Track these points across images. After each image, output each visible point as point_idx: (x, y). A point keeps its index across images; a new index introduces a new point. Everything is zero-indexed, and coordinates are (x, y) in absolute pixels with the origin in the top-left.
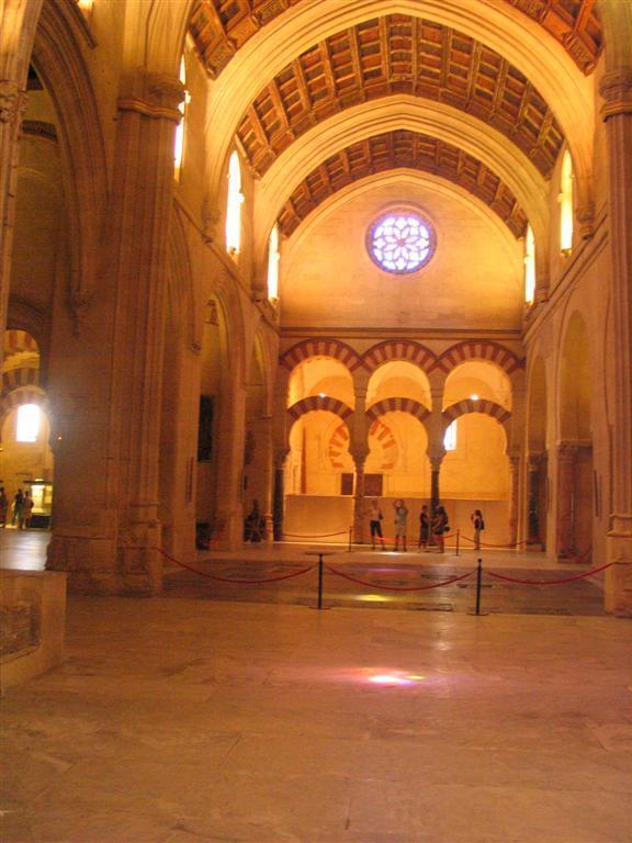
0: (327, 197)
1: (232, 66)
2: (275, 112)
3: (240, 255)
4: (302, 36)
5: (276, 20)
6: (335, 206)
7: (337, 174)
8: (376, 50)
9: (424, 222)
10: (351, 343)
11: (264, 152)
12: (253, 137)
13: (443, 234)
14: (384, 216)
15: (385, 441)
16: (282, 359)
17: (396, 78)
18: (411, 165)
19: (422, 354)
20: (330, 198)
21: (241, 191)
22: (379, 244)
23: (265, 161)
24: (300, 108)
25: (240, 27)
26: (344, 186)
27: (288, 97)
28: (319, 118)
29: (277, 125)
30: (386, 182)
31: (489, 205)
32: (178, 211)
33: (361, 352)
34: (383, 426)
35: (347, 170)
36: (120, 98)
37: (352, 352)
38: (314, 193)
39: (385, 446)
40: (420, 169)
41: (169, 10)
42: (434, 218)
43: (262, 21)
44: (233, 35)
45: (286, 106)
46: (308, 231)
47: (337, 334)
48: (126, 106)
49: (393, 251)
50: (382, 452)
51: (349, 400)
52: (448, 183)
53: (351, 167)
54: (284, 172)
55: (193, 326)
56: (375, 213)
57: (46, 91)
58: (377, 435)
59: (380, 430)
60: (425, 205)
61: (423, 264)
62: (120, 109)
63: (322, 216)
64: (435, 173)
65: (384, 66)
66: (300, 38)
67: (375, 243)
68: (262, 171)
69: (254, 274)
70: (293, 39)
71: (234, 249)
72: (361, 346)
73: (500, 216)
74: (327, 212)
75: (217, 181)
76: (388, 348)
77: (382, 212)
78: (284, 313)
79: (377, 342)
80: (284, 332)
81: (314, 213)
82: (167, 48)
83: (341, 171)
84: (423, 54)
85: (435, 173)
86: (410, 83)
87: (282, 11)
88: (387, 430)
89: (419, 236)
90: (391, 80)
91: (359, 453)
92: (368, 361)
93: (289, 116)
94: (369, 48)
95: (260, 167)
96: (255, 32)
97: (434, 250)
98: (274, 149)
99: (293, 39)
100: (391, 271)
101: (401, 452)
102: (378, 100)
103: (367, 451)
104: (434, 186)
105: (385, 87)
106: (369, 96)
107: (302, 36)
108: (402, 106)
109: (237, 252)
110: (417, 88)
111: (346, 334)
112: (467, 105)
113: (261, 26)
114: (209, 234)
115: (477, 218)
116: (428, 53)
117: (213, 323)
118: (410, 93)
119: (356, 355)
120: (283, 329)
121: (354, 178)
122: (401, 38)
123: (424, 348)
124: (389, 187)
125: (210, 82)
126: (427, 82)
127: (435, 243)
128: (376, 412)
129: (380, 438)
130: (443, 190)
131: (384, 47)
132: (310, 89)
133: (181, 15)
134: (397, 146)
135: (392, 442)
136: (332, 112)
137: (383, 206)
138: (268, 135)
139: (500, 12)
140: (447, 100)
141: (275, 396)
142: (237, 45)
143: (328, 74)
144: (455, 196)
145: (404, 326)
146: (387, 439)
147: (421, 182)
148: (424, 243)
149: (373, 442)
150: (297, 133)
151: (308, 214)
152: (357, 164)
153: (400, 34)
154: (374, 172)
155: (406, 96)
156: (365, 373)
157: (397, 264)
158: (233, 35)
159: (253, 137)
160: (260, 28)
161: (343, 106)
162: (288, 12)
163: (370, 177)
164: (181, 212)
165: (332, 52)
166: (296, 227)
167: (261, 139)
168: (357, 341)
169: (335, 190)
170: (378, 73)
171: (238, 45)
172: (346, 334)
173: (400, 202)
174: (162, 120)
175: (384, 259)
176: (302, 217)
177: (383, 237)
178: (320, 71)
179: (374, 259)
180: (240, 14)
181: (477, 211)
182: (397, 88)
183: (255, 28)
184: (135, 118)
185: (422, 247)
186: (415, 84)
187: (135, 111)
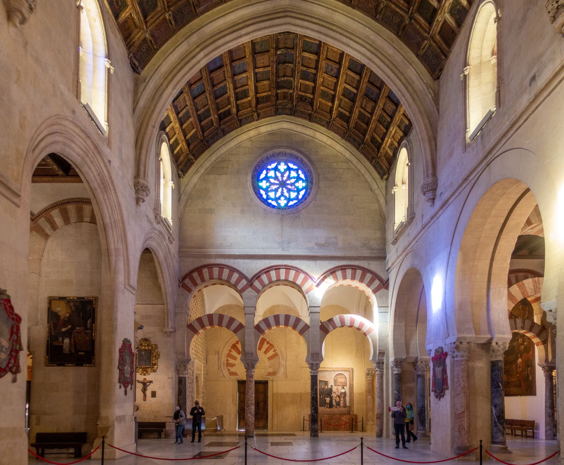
0: (217, 140)
15: (271, 353)
31: (358, 149)
34: (268, 343)
39: (270, 358)
50: (267, 363)
51: (240, 319)
52: (323, 129)
58: (264, 349)
59: (265, 346)
67: (261, 184)
73: (368, 159)
88: (271, 346)
91: (250, 364)
100: (274, 207)
101: (283, 363)
103: (257, 360)
119: (246, 278)
128: (263, 326)
129: (266, 352)
130: (318, 136)
135: (276, 355)
137: (266, 151)
141: (176, 314)
146: (271, 353)
148: (301, 185)
149: (261, 354)
156: (255, 294)
157: (279, 201)
163: (255, 123)
177: (267, 178)
179: (260, 196)
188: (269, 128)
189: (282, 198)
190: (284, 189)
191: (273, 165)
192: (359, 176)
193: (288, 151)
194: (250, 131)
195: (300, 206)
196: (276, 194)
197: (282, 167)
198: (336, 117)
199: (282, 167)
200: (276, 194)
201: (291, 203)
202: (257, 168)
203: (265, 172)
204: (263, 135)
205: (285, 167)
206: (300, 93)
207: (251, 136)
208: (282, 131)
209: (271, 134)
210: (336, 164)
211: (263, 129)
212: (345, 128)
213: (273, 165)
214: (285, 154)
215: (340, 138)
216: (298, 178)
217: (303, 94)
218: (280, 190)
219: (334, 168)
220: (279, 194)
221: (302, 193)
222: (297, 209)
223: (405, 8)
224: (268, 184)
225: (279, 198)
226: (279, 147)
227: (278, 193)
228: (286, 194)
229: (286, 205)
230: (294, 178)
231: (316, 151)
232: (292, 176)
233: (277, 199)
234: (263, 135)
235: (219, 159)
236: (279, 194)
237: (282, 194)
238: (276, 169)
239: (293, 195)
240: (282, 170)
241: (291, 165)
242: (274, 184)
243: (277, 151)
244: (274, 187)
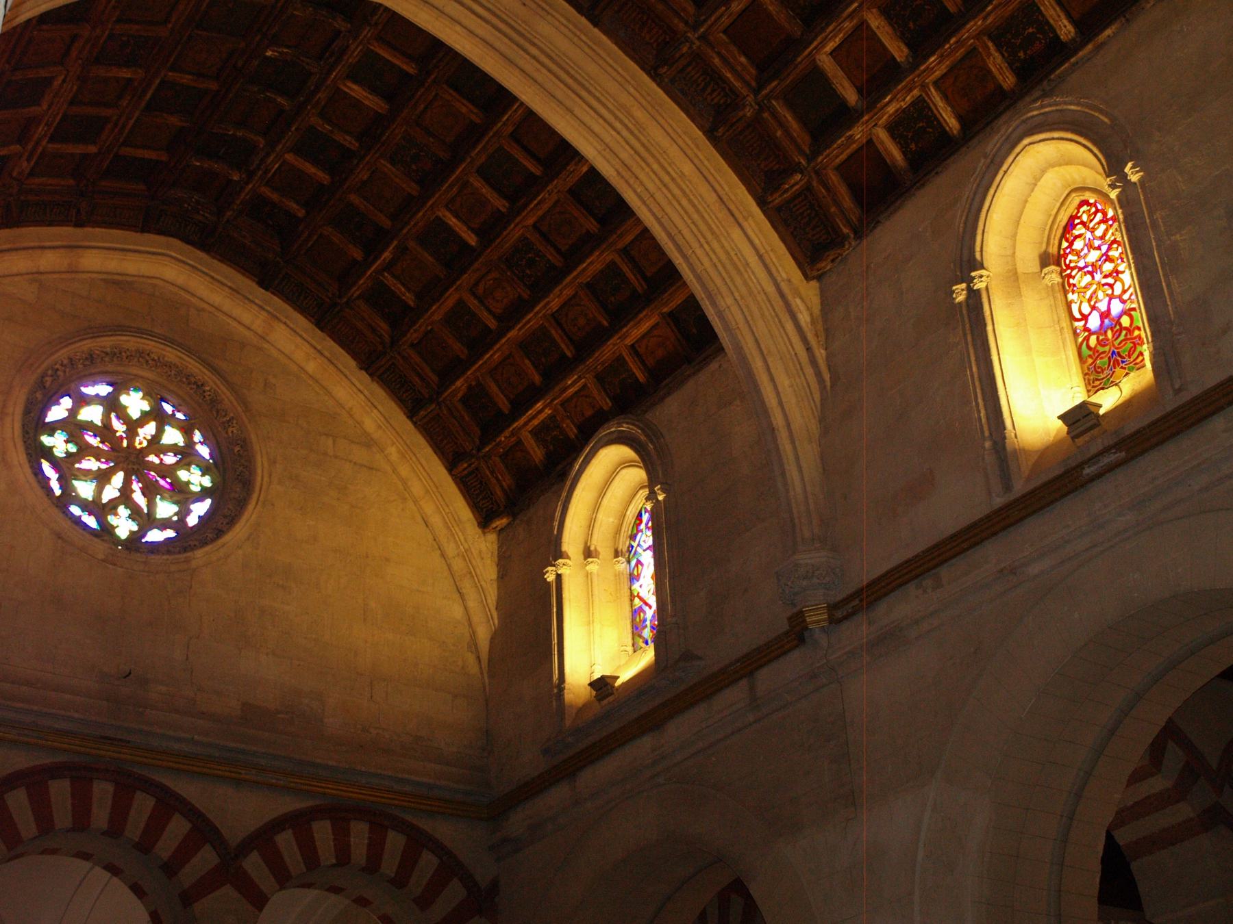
14: (91, 368)
31: (411, 415)
49: (102, 478)
85: (263, 284)
97: (242, 504)
115: (368, 442)
124: (119, 283)
147: (218, 298)
173: (150, 334)
175: (69, 496)
181: (370, 423)
189: (123, 511)
191: (104, 390)
192: (404, 499)
194: (47, 251)
196: (99, 491)
197: (135, 403)
198: (358, 297)
200: (99, 491)
201: (155, 536)
203: (67, 402)
204: (85, 276)
205: (146, 406)
207: (42, 269)
208: (155, 286)
209: (115, 282)
210: (330, 442)
212: (381, 336)
214: (159, 364)
215: (352, 363)
216: (186, 455)
217: (275, 197)
218: (118, 479)
219: (325, 454)
220: (111, 492)
221: (200, 509)
222: (187, 561)
223: (748, 78)
225: (112, 506)
226: (140, 332)
227: (108, 488)
228: (139, 498)
229: (135, 538)
230: (174, 449)
231: (266, 384)
233: (99, 509)
234: (85, 276)
236: (111, 492)
237: (125, 495)
240: (135, 414)
242: (97, 454)
243: (130, 343)
244: (90, 464)
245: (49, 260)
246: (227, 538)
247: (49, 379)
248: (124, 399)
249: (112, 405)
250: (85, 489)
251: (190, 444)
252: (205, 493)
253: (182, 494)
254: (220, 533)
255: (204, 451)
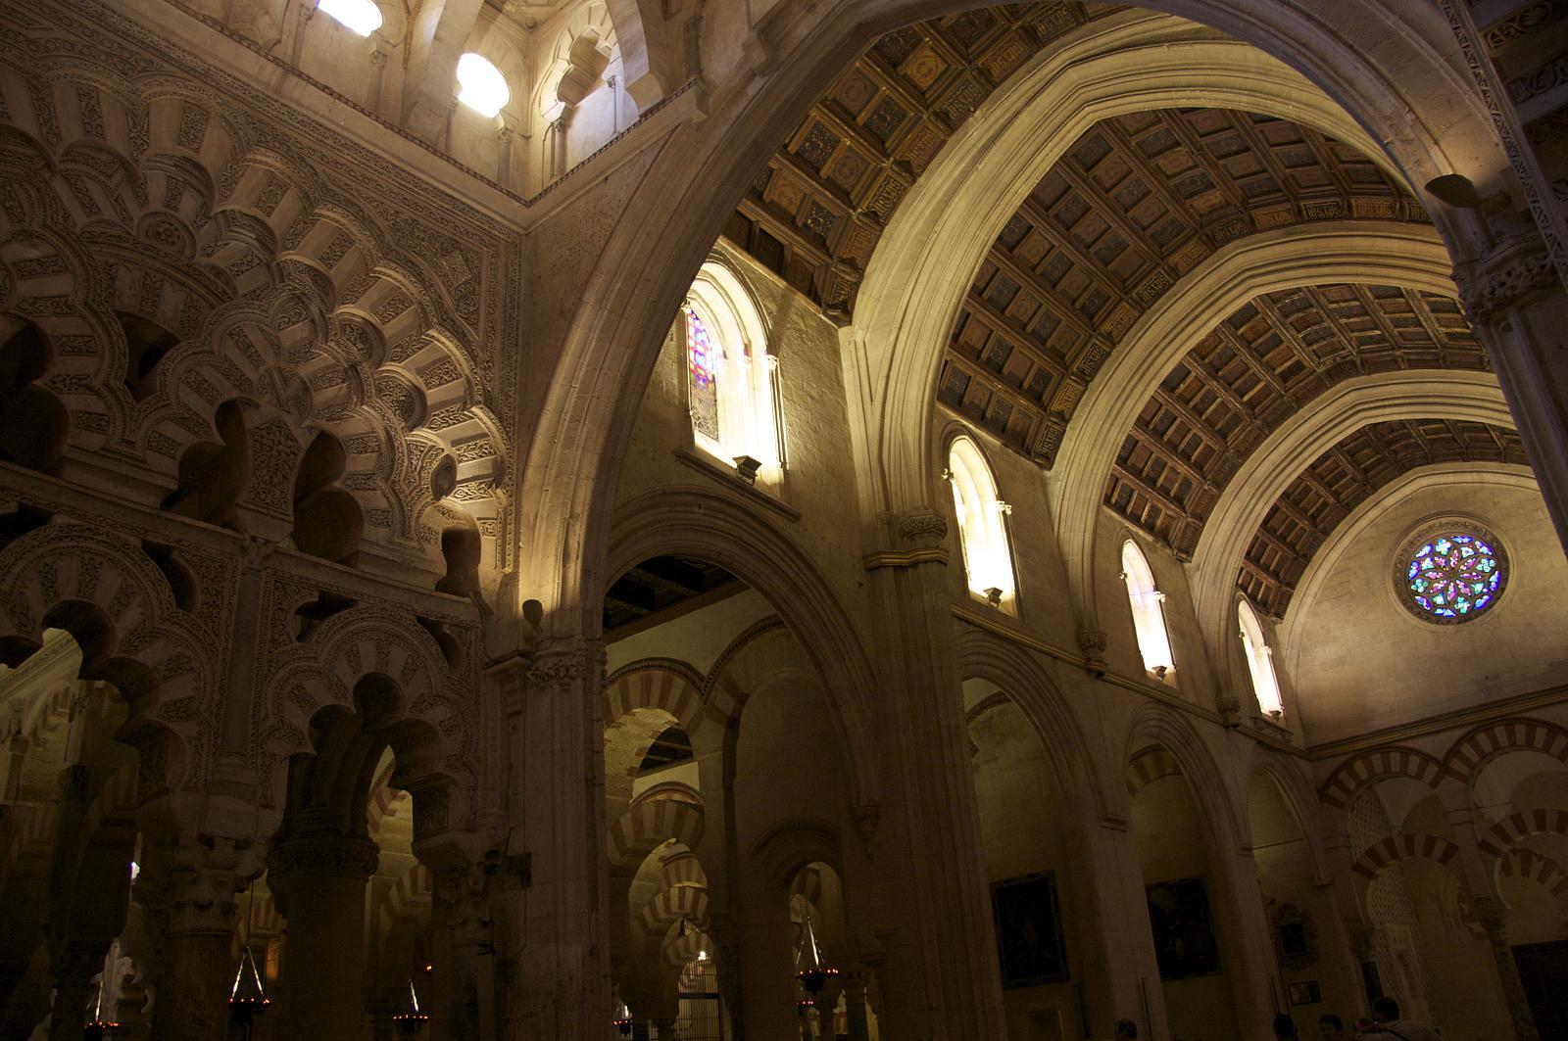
0: (1318, 546)
1: (1066, 446)
2: (1173, 469)
3: (1177, 674)
4: (1142, 376)
5: (1104, 368)
6: (1334, 555)
7: (1320, 510)
8: (1277, 341)
9: (1475, 534)
10: (1418, 744)
11: (1181, 524)
12: (1155, 512)
13: (1513, 541)
14: (1414, 546)
16: (1323, 794)
17: (1328, 361)
18: (1428, 460)
19: (1541, 733)
20: (1323, 546)
21: (1157, 588)
22: (1420, 586)
23: (1189, 534)
24: (1209, 450)
25: (1060, 395)
26: (1339, 522)
27: (1182, 446)
28: (1244, 454)
29: (1186, 484)
30: (1398, 496)
32: (1026, 653)
33: (1440, 755)
35: (1331, 500)
36: (864, 558)
37: (1426, 758)
38: (1298, 548)
40: (1441, 462)
41: (903, 434)
42: (1489, 523)
43: (1085, 378)
44: (1055, 407)
45: (1186, 456)
46: (1309, 600)
47: (1395, 736)
48: (874, 564)
52: (1493, 465)
53: (1337, 495)
54: (1219, 540)
55: (1100, 793)
56: (1396, 544)
57: (753, 589)
60: (1469, 509)
61: (1495, 595)
62: (869, 570)
63: (1321, 574)
64: (1465, 458)
65: (1302, 354)
66: (1139, 381)
68: (1188, 551)
69: (1218, 690)
70: (1132, 383)
71: (1163, 669)
72: (1436, 745)
74: (1327, 565)
75: (1088, 592)
76: (1482, 738)
77: (1406, 541)
78: (1307, 726)
79: (1458, 733)
80: (1313, 753)
81: (1308, 573)
82: (909, 476)
83: (1325, 504)
84: (1343, 321)
86: (1353, 363)
87: (1108, 354)
89: (1477, 555)
90: (1322, 369)
92: (1456, 765)
93: (1198, 466)
94: (1266, 342)
95: (1184, 546)
96: (1083, 392)
97: (1507, 569)
98: (1194, 515)
99: (1132, 383)
100: (1448, 620)
102: (1318, 399)
104: (1474, 477)
105: (1319, 379)
106: (1301, 401)
107: (1142, 376)
108: (1353, 395)
109: (1170, 669)
110: (1362, 364)
111: (1408, 733)
112: (1444, 358)
113: (1087, 383)
114: (1095, 666)
116: (1348, 317)
117: (1178, 774)
118: (1358, 374)
120: (1311, 750)
121: (1349, 508)
122: (1301, 315)
123: (1544, 723)
124: (1406, 502)
125: (1047, 474)
126: (1372, 351)
127: (1506, 559)
130: (1488, 477)
131: (1286, 335)
132: (1210, 423)
133: (917, 435)
134: (1390, 443)
136: (1258, 440)
138: (1179, 501)
139: (1391, 237)
140: (1413, 364)
142: (1064, 419)
143: (1223, 396)
144: (1513, 480)
145: (1497, 698)
147: (1451, 478)
148: (1486, 565)
150: (1221, 485)
151: (1299, 577)
152: (1346, 487)
153: (1299, 310)
154: (1375, 490)
155: (1353, 379)
158: (1055, 407)
159: (1155, 512)
160: (1087, 386)
161: (1271, 426)
162: (1114, 353)
164: (1032, 652)
165: (1214, 370)
166: (1288, 602)
167: (1168, 509)
168: (1429, 739)
169: (1327, 533)
170: (1299, 367)
171: (1067, 417)
172: (1408, 733)
174: (921, 565)
176: (1292, 585)
178: (1211, 397)
180: (1056, 378)
182: (1339, 372)
183: (1082, 389)
184: (888, 575)
185: (1487, 569)
186: (1358, 361)
187: (884, 566)
188: (1398, 496)
190: (1458, 582)
191: (1426, 550)
193: (1444, 520)
195: (1497, 607)
197: (1443, 547)
199: (1443, 547)
201: (1479, 602)
202: (1399, 566)
205: (1449, 545)
206: (1428, 437)
211: (1389, 502)
213: (1426, 550)
218: (1451, 588)
224: (1426, 584)
232: (1465, 555)
235: (1332, 572)
238: (1433, 554)
239: (1478, 587)
241: (1459, 540)
243: (1424, 526)
245: (1372, 515)
246: (1505, 593)
247: (1399, 566)
248: (1438, 549)
249: (1433, 554)
250: (1439, 600)
251: (1476, 551)
252: (1492, 572)
253: (1483, 577)
254: (1503, 590)
255: (1484, 550)
